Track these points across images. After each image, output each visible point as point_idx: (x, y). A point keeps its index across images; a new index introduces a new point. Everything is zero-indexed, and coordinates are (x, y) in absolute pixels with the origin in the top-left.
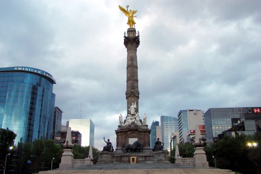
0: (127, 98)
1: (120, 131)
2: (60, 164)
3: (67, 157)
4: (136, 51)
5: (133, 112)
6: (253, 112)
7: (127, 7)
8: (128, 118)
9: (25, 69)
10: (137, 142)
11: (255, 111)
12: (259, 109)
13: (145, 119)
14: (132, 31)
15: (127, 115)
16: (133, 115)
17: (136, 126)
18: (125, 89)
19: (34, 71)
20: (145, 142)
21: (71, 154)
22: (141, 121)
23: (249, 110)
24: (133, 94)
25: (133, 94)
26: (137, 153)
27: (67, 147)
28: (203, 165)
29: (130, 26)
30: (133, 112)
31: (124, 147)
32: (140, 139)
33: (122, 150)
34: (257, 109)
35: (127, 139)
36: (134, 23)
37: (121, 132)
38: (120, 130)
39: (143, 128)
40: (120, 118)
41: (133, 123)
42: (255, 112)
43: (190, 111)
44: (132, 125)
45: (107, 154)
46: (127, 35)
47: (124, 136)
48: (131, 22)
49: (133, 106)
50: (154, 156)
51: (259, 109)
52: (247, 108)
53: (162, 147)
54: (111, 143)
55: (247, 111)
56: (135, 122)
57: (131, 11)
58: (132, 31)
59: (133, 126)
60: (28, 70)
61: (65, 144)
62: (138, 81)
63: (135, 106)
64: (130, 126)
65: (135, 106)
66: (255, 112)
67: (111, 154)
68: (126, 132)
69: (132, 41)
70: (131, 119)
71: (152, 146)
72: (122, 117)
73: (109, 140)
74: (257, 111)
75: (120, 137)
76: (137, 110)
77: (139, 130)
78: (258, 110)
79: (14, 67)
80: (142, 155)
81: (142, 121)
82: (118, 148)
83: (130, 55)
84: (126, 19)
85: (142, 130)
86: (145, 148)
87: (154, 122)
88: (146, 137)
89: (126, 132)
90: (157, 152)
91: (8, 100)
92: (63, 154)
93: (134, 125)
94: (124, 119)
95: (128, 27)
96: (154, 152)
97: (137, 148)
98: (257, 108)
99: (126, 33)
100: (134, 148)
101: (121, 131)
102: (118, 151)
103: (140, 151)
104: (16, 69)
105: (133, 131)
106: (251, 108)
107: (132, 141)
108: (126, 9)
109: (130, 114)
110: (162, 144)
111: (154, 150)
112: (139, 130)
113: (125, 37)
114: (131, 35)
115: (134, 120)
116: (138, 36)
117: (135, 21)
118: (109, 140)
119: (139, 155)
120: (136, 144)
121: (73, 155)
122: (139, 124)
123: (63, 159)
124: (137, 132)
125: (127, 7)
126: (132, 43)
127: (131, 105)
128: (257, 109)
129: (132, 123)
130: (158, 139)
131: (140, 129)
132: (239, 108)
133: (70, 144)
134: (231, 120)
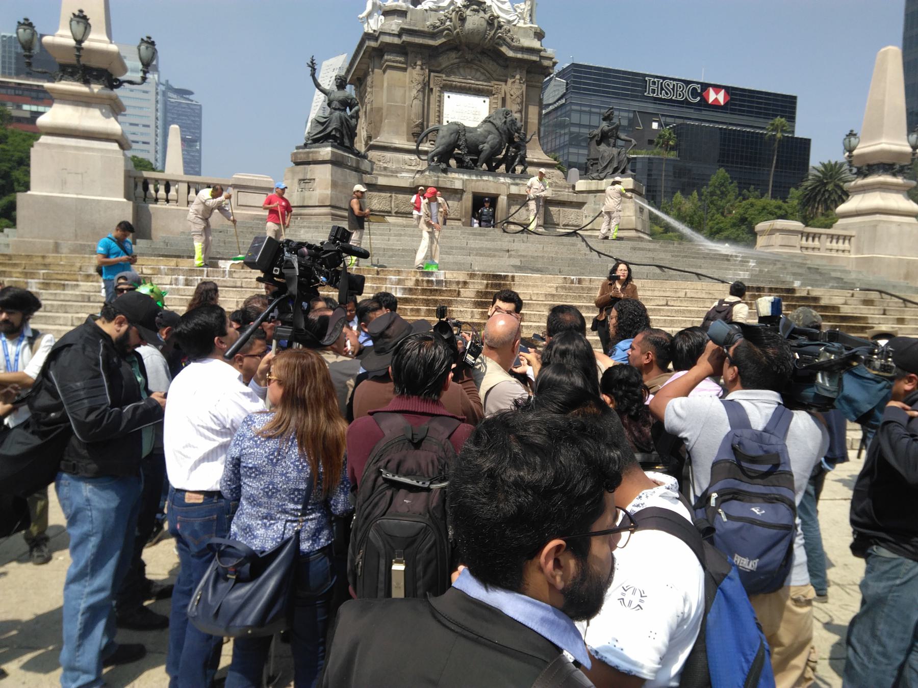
1: (396, 41)
2: (21, 198)
6: (704, 100)
11: (712, 96)
12: (722, 92)
23: (694, 93)
26: (502, 180)
33: (417, 152)
34: (717, 93)
35: (434, 97)
37: (402, 50)
38: (403, 31)
42: (711, 100)
44: (468, 12)
47: (415, 74)
51: (722, 92)
52: (687, 83)
55: (686, 95)
66: (711, 100)
74: (716, 100)
77: (502, 55)
78: (721, 97)
85: (519, 56)
93: (482, 14)
98: (717, 88)
100: (486, 147)
101: (405, 38)
102: (388, 155)
103: (514, 170)
105: (469, 56)
106: (702, 84)
112: (504, 49)
119: (514, 190)
123: (42, 154)
124: (491, 66)
128: (717, 93)
131: (510, 47)
132: (664, 78)
134: (631, 115)
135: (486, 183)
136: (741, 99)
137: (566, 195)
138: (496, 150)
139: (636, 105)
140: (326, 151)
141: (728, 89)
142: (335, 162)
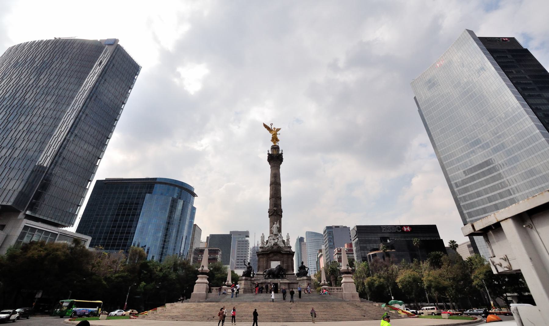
0: (270, 216)
3: (201, 285)
4: (279, 168)
5: (275, 231)
6: (403, 231)
7: (271, 124)
8: (270, 238)
11: (405, 229)
13: (288, 240)
14: (275, 148)
15: (269, 235)
17: (279, 247)
18: (268, 207)
20: (288, 266)
21: (206, 281)
22: (283, 241)
24: (276, 213)
25: (276, 213)
27: (203, 273)
28: (353, 297)
31: (265, 272)
32: (283, 262)
33: (263, 275)
36: (277, 140)
37: (263, 254)
39: (286, 250)
40: (263, 237)
41: (276, 244)
43: (336, 227)
46: (270, 153)
48: (275, 139)
49: (276, 226)
50: (298, 283)
53: (307, 272)
57: (275, 128)
58: (275, 148)
59: (275, 247)
61: (200, 269)
62: (280, 198)
63: (278, 225)
64: (272, 247)
65: (278, 225)
67: (251, 280)
68: (268, 254)
69: (275, 158)
70: (274, 239)
71: (295, 272)
72: (264, 237)
75: (261, 259)
76: (279, 230)
78: (408, 229)
80: (285, 282)
81: (286, 241)
82: (259, 273)
84: (270, 136)
86: (289, 273)
88: (290, 259)
89: (268, 254)
90: (301, 279)
92: (197, 281)
94: (266, 239)
95: (272, 144)
96: (298, 279)
98: (406, 226)
99: (270, 150)
107: (274, 265)
108: (270, 127)
109: (272, 233)
110: (307, 269)
111: (298, 275)
113: (268, 154)
114: (275, 153)
115: (276, 241)
116: (282, 154)
119: (281, 282)
120: (280, 268)
121: (208, 282)
122: (281, 246)
123: (196, 287)
125: (271, 124)
127: (274, 224)
129: (274, 244)
130: (302, 263)
133: (206, 268)
135: (276, 281)
136: (416, 229)
137: (294, 281)
138: (278, 273)
139: (380, 235)
140: (244, 278)
141: (410, 226)
142: (245, 280)
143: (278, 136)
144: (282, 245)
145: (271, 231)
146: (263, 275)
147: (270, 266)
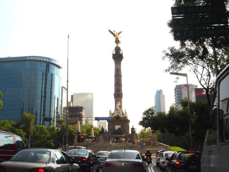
0: (115, 98)
4: (120, 64)
5: (118, 108)
9: (36, 59)
10: (119, 128)
14: (118, 49)
16: (118, 110)
19: (43, 59)
22: (123, 113)
24: (118, 95)
29: (117, 44)
30: (118, 108)
32: (122, 126)
40: (110, 111)
45: (101, 136)
48: (117, 41)
49: (119, 104)
54: (104, 129)
56: (119, 115)
57: (117, 33)
58: (118, 49)
60: (38, 59)
69: (118, 57)
70: (117, 113)
73: (102, 127)
76: (121, 107)
79: (26, 57)
83: (117, 67)
87: (159, 90)
91: (54, 122)
97: (120, 132)
104: (28, 58)
107: (117, 127)
108: (113, 32)
110: (135, 130)
115: (118, 114)
116: (122, 54)
117: (119, 40)
118: (102, 127)
126: (118, 59)
127: (117, 103)
130: (133, 126)
143: (119, 39)
144: (121, 116)
145: (115, 107)
146: (111, 133)
147: (115, 128)
